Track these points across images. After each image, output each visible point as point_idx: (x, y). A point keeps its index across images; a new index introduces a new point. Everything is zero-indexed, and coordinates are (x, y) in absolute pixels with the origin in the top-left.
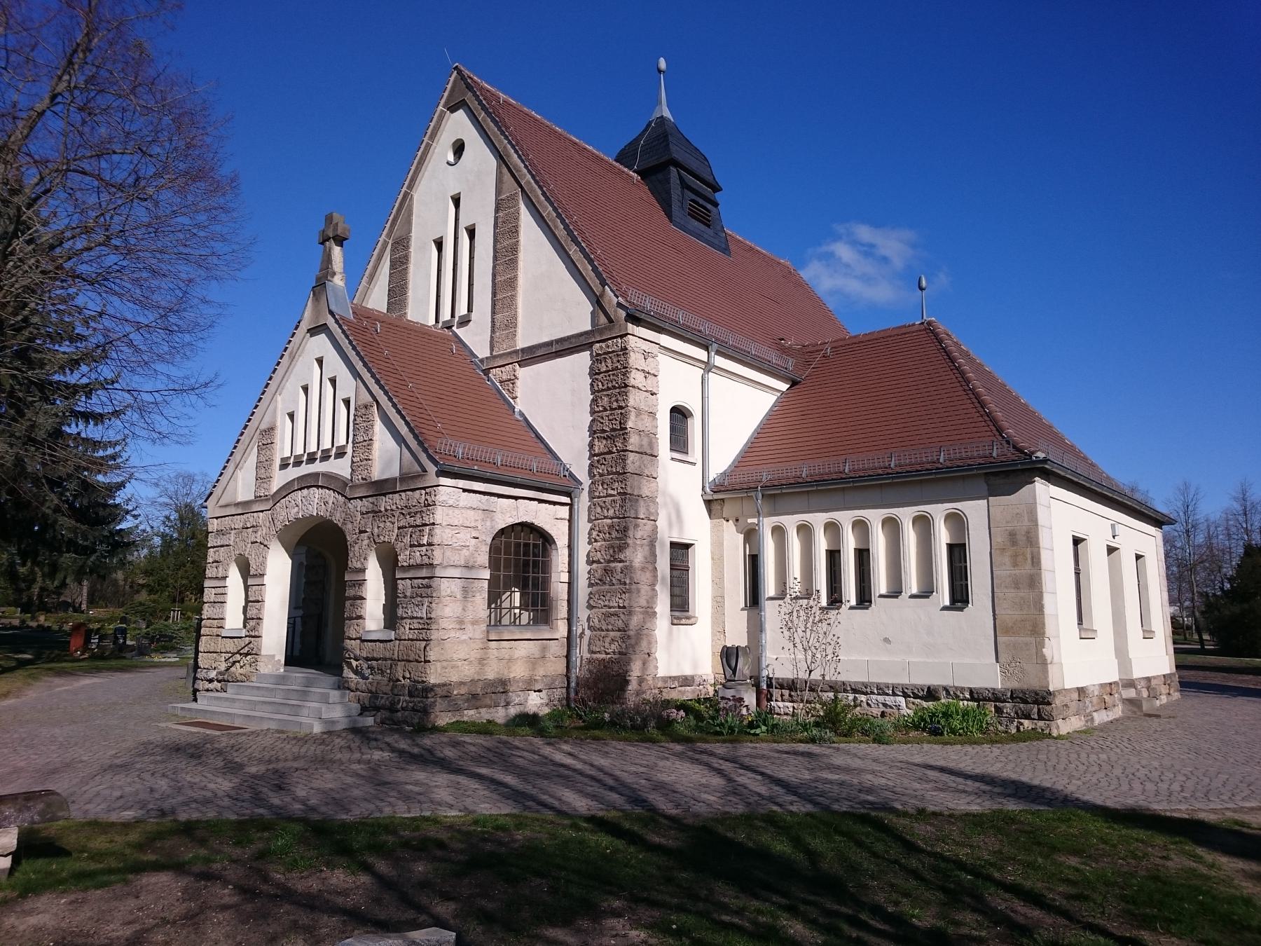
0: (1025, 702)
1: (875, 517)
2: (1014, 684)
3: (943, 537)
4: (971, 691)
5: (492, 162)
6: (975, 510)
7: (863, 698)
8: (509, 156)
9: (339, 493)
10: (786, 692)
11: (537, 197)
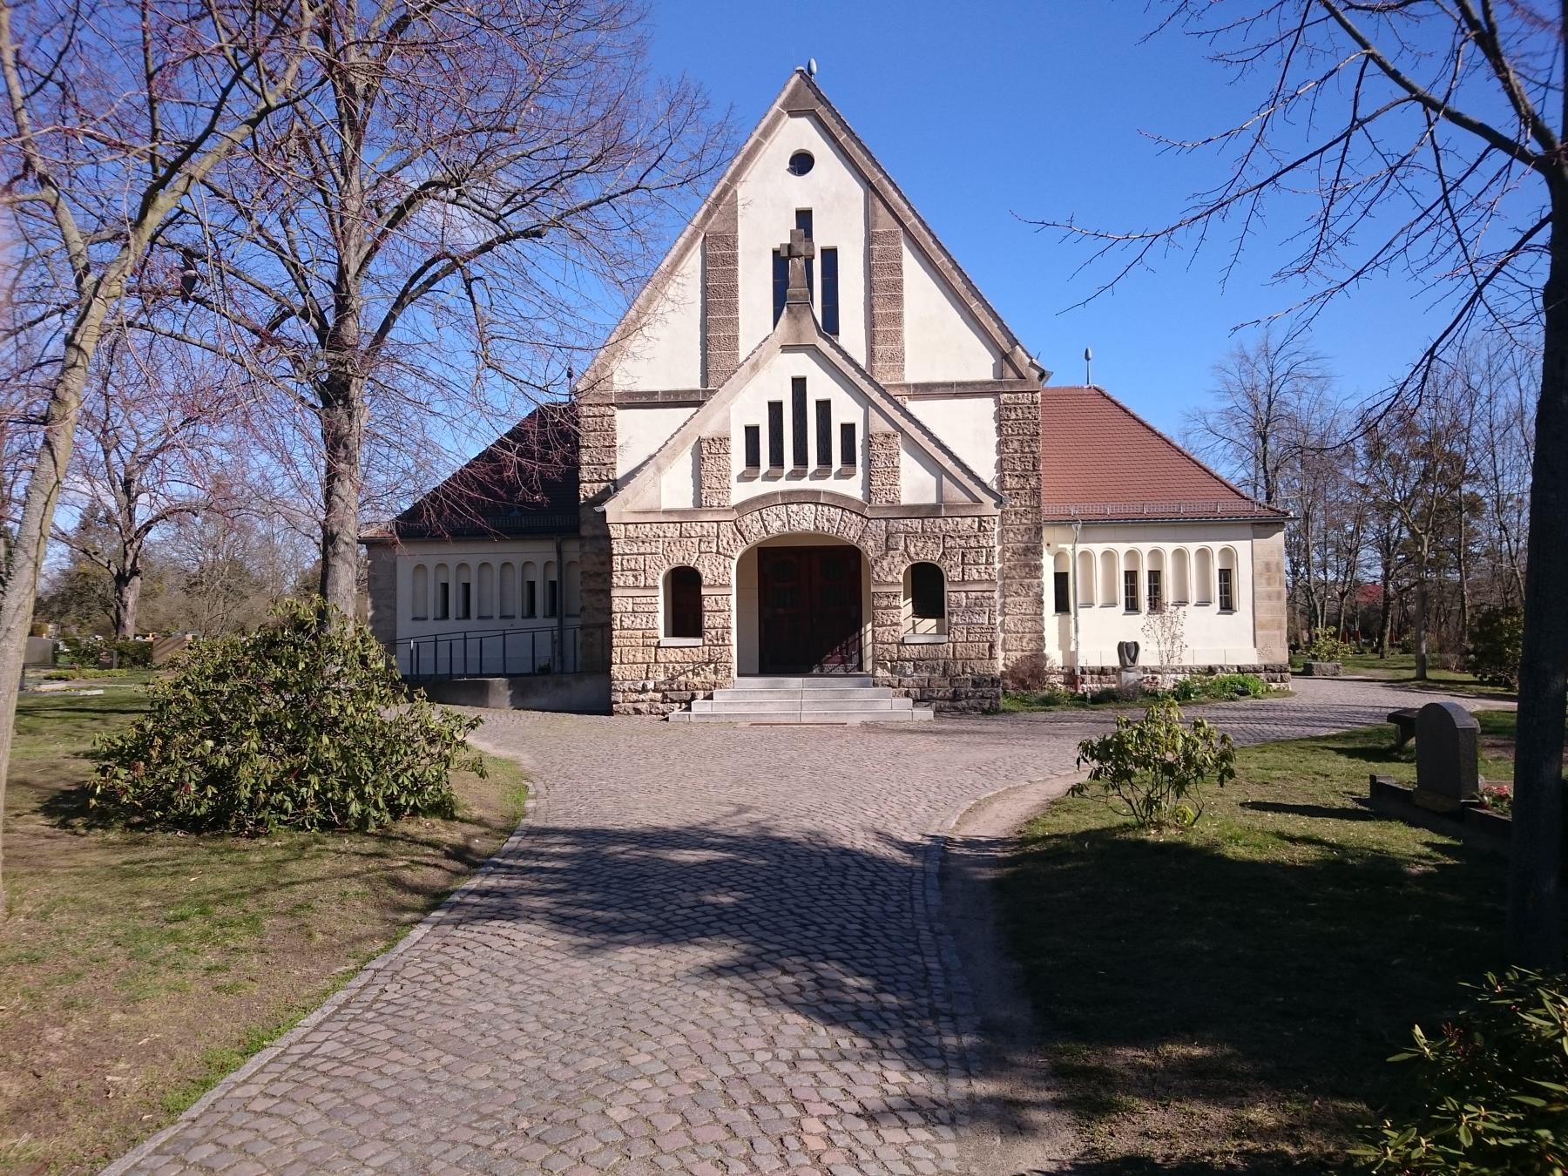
0: (1273, 671)
1: (1168, 548)
2: (1266, 662)
3: (1216, 565)
4: (1239, 668)
5: (858, 191)
6: (1242, 548)
7: (1159, 677)
8: (886, 192)
9: (857, 514)
10: (1096, 676)
11: (927, 243)
